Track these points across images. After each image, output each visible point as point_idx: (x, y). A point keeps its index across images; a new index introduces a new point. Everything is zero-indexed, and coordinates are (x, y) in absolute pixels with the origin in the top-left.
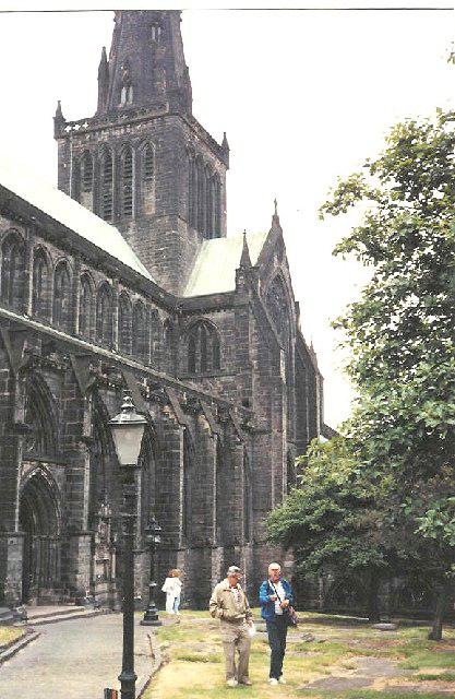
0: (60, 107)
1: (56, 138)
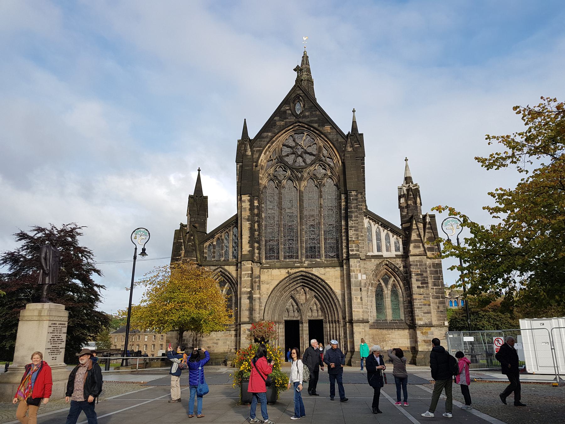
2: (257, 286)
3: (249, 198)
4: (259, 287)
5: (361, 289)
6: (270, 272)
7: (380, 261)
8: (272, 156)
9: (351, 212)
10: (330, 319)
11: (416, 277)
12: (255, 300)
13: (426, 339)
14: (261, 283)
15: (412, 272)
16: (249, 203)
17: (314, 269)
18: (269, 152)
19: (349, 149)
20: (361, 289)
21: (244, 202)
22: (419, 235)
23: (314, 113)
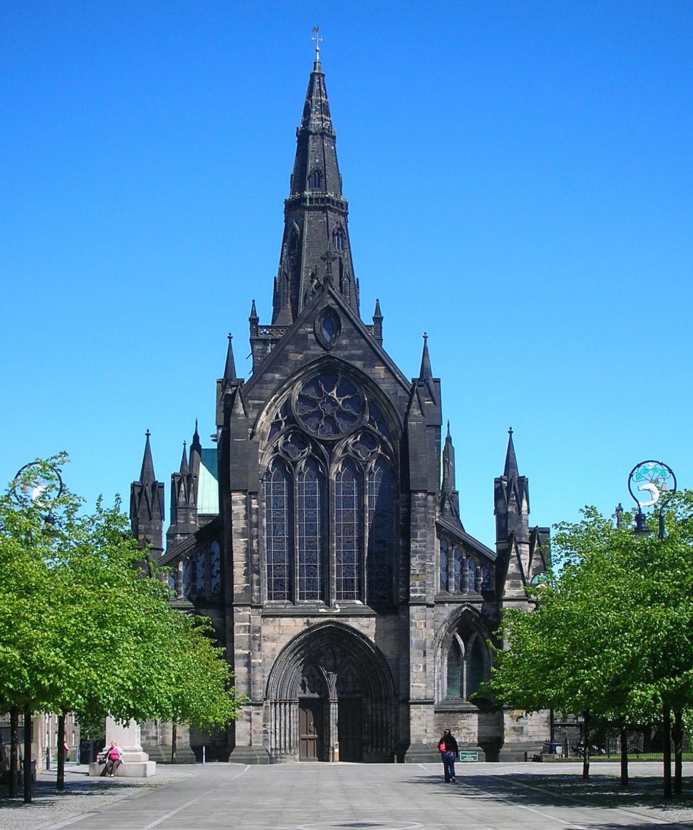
0: (254, 305)
2: (257, 645)
3: (245, 496)
4: (260, 645)
5: (425, 652)
8: (280, 415)
9: (416, 527)
12: (253, 667)
14: (262, 639)
16: (244, 506)
17: (350, 619)
18: (276, 407)
19: (416, 412)
20: (425, 652)
21: (236, 503)
22: (520, 566)
23: (356, 341)
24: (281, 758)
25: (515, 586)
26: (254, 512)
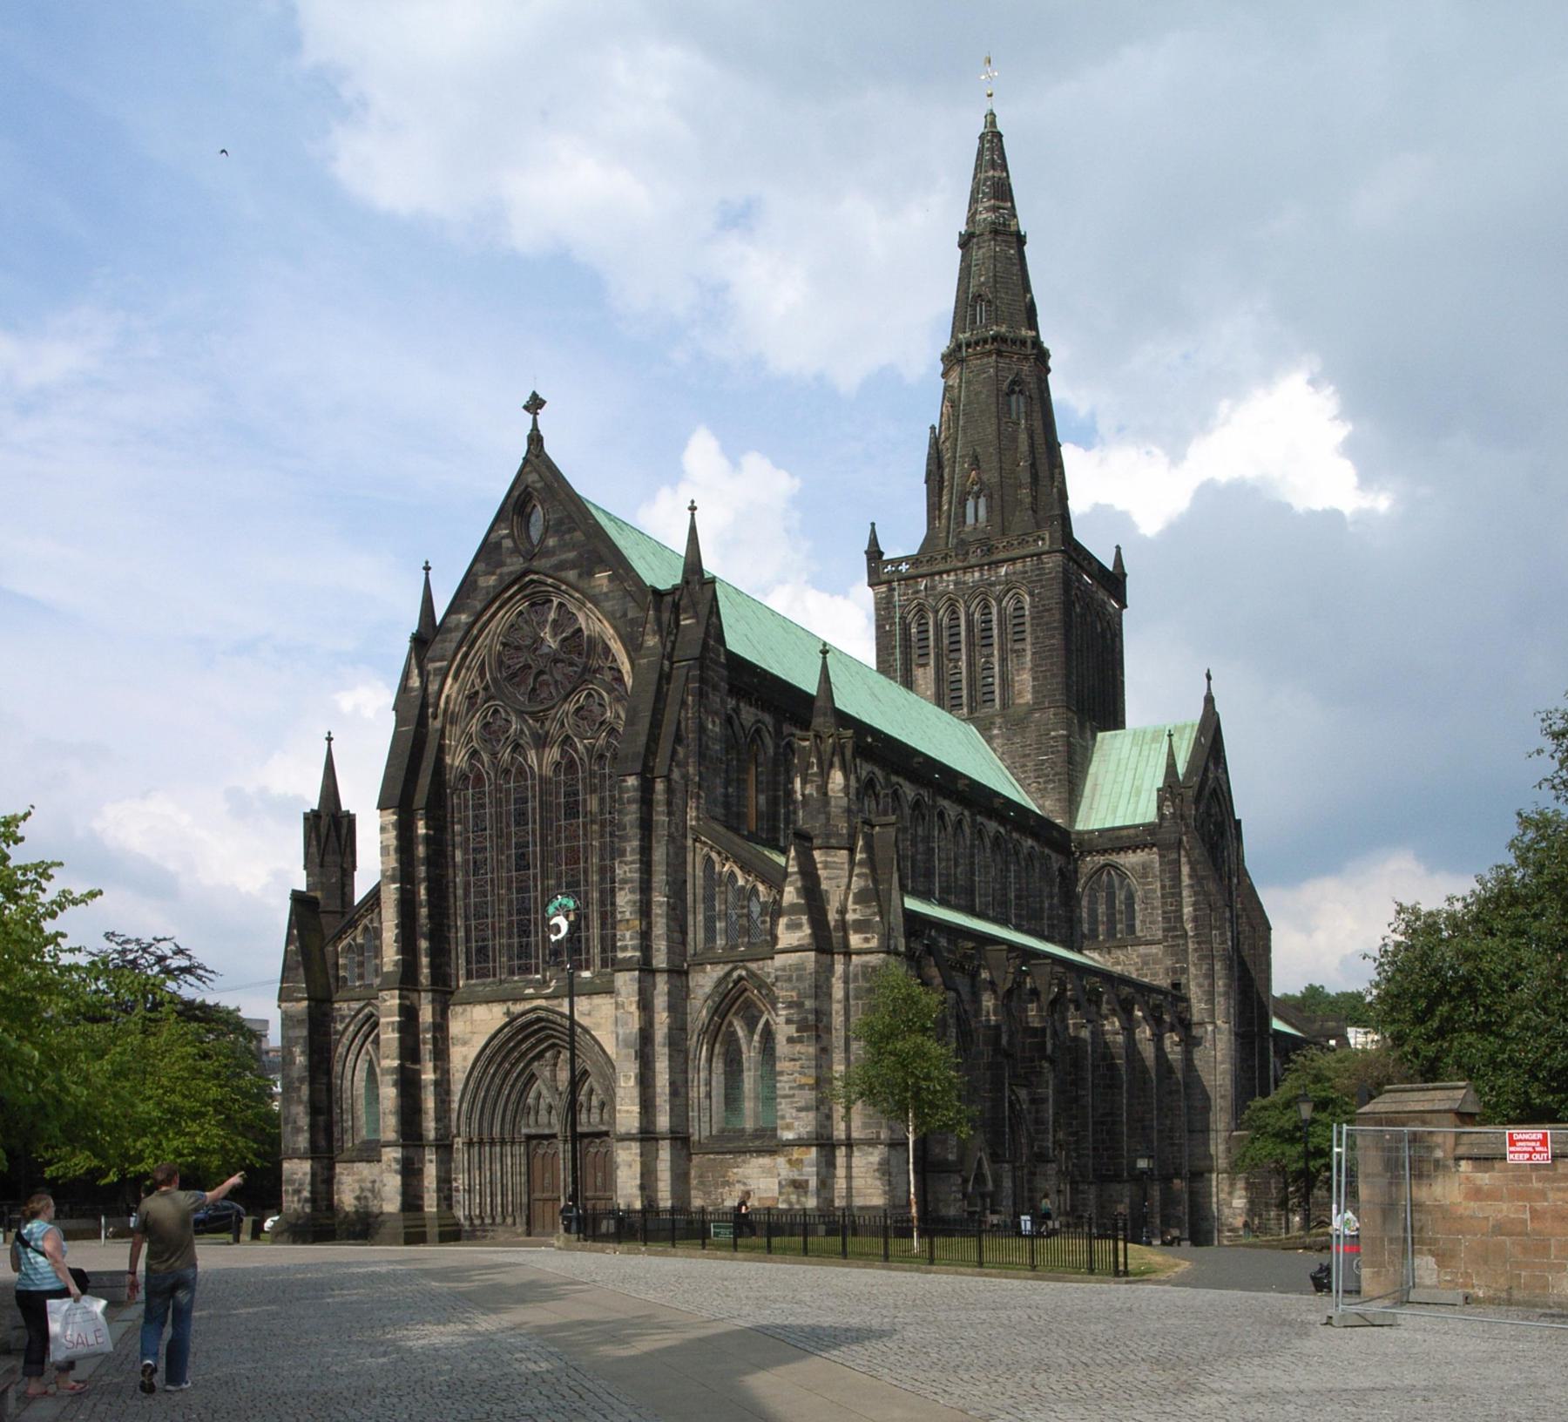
0: (873, 531)
1: (871, 585)
3: (395, 817)
6: (468, 1014)
7: (728, 967)
10: (506, 1132)
11: (784, 1013)
13: (797, 1177)
15: (778, 998)
24: (485, 1231)
25: (789, 927)
26: (420, 840)
